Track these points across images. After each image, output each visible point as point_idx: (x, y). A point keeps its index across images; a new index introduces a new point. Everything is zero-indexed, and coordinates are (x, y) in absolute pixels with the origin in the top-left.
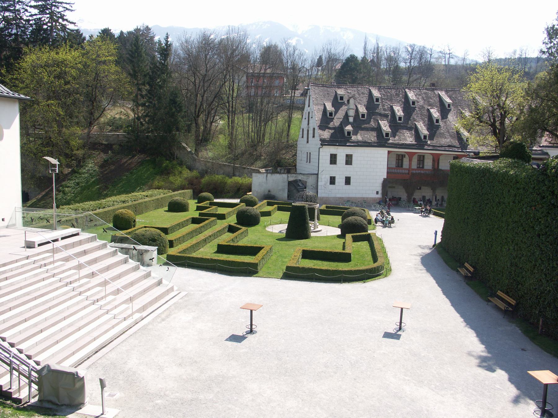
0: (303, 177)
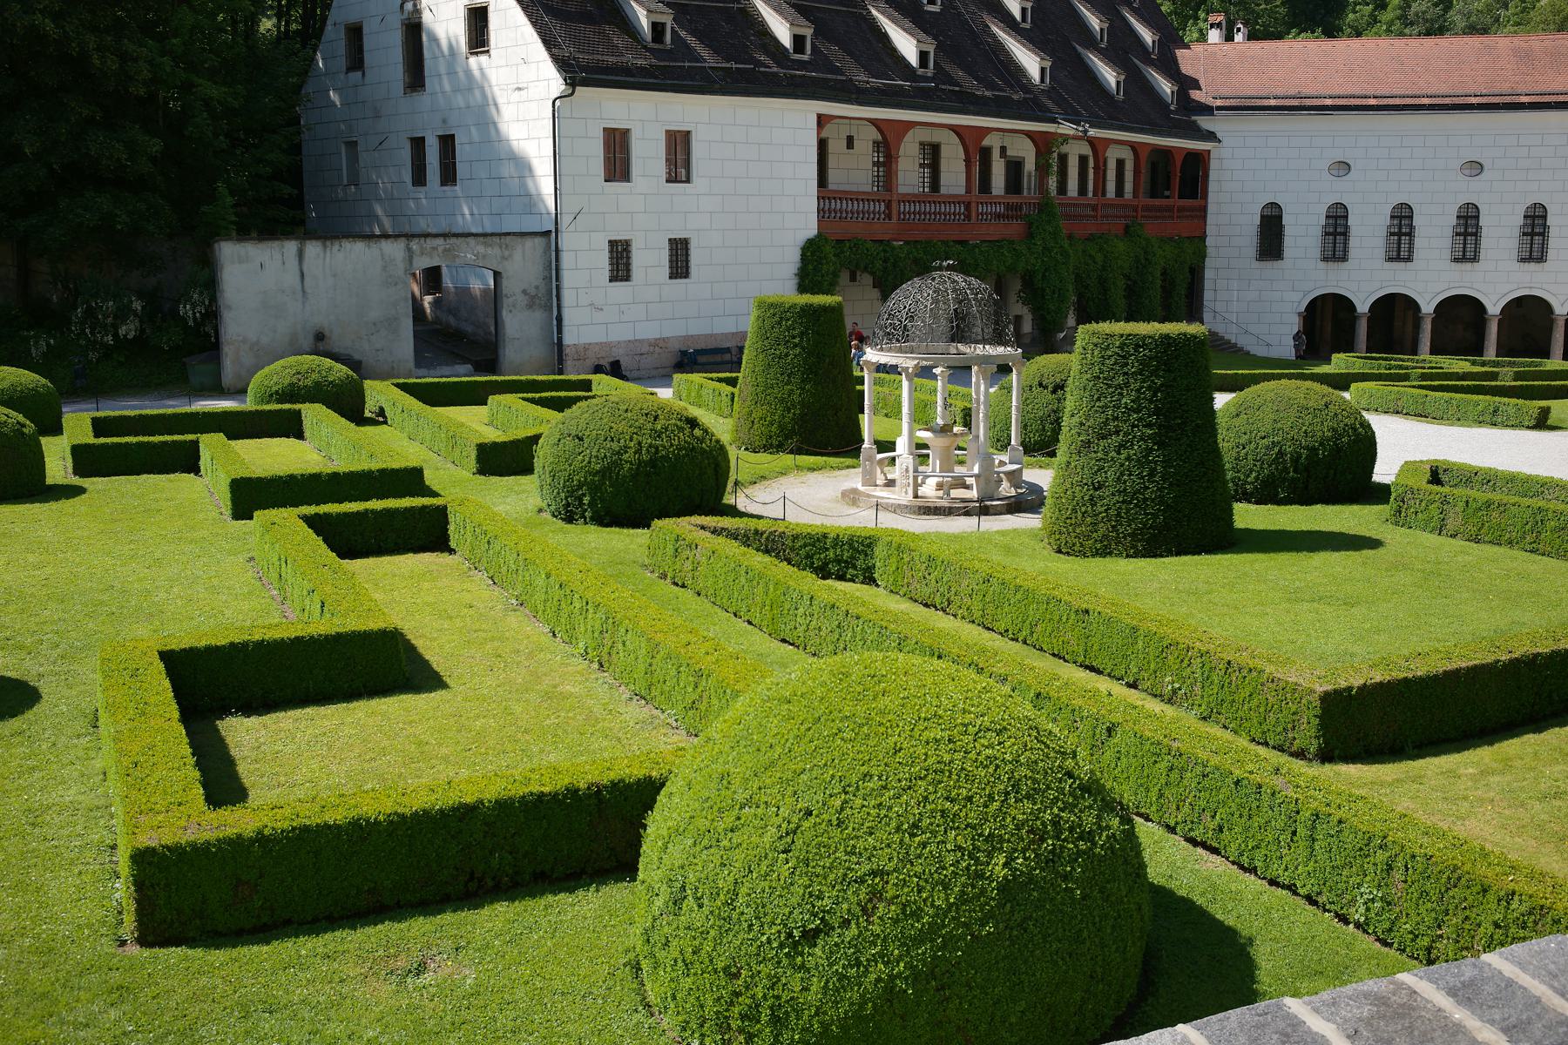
0: (481, 249)
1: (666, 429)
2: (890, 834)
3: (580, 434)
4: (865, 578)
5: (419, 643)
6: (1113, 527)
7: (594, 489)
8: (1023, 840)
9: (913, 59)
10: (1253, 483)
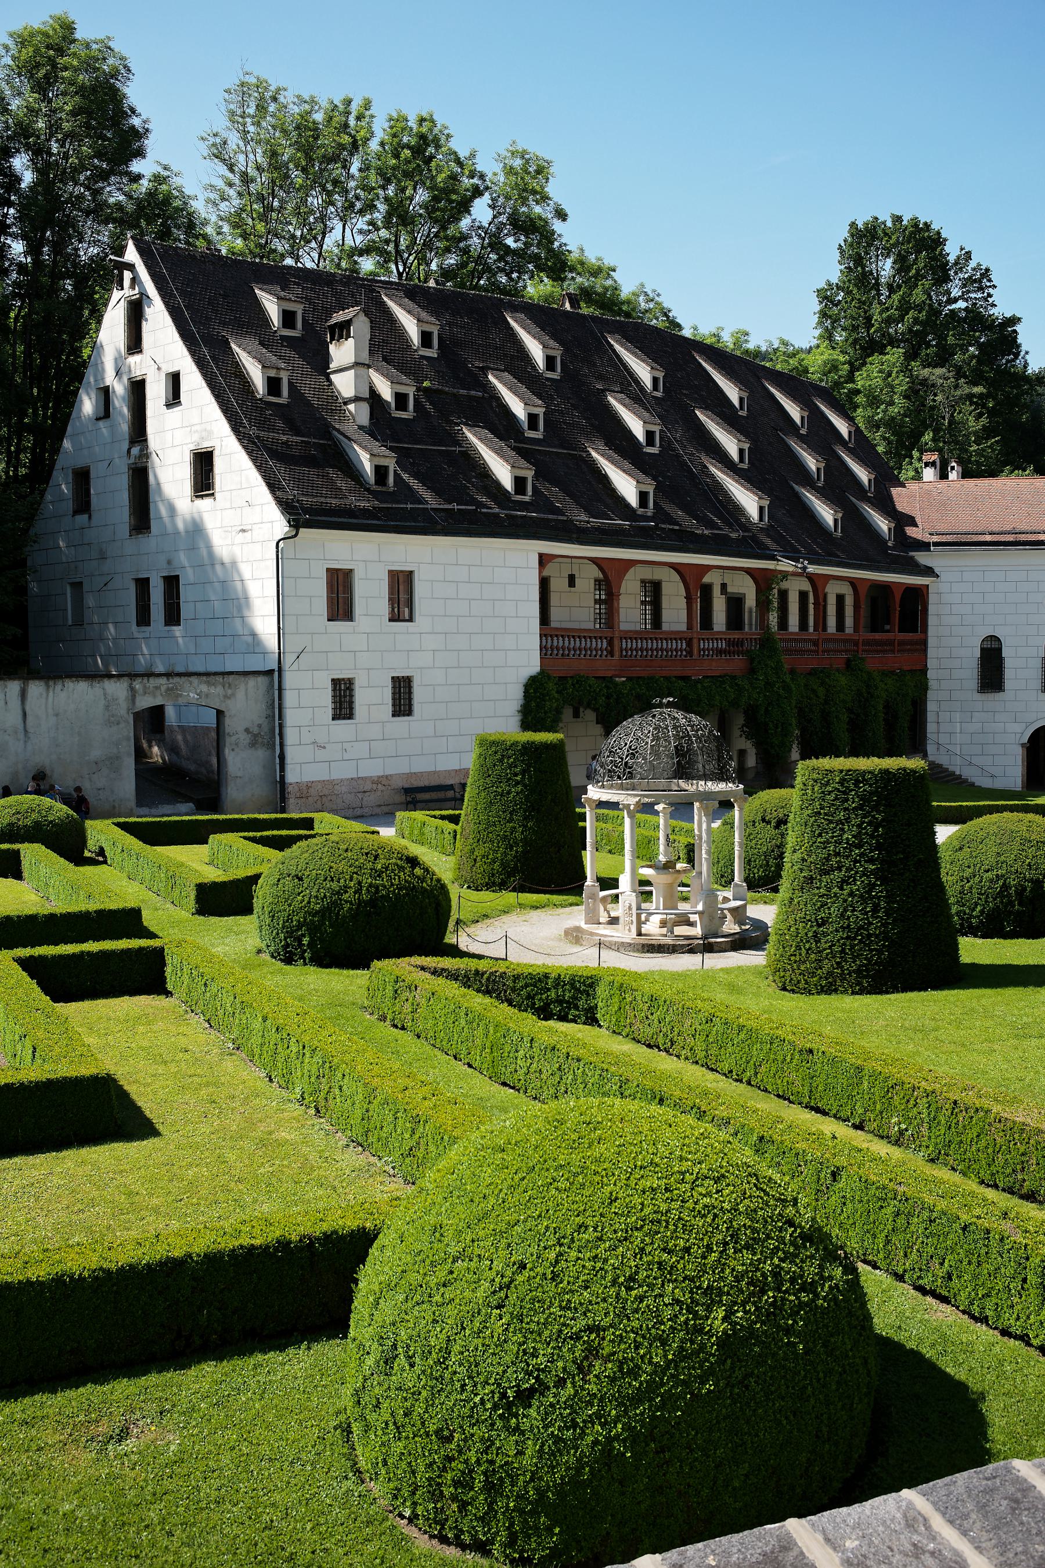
0: (204, 688)
1: (387, 868)
2: (605, 1287)
3: (300, 874)
4: (587, 1018)
5: (133, 1090)
6: (838, 963)
7: (313, 930)
8: (743, 1292)
9: (633, 499)
10: (978, 917)
